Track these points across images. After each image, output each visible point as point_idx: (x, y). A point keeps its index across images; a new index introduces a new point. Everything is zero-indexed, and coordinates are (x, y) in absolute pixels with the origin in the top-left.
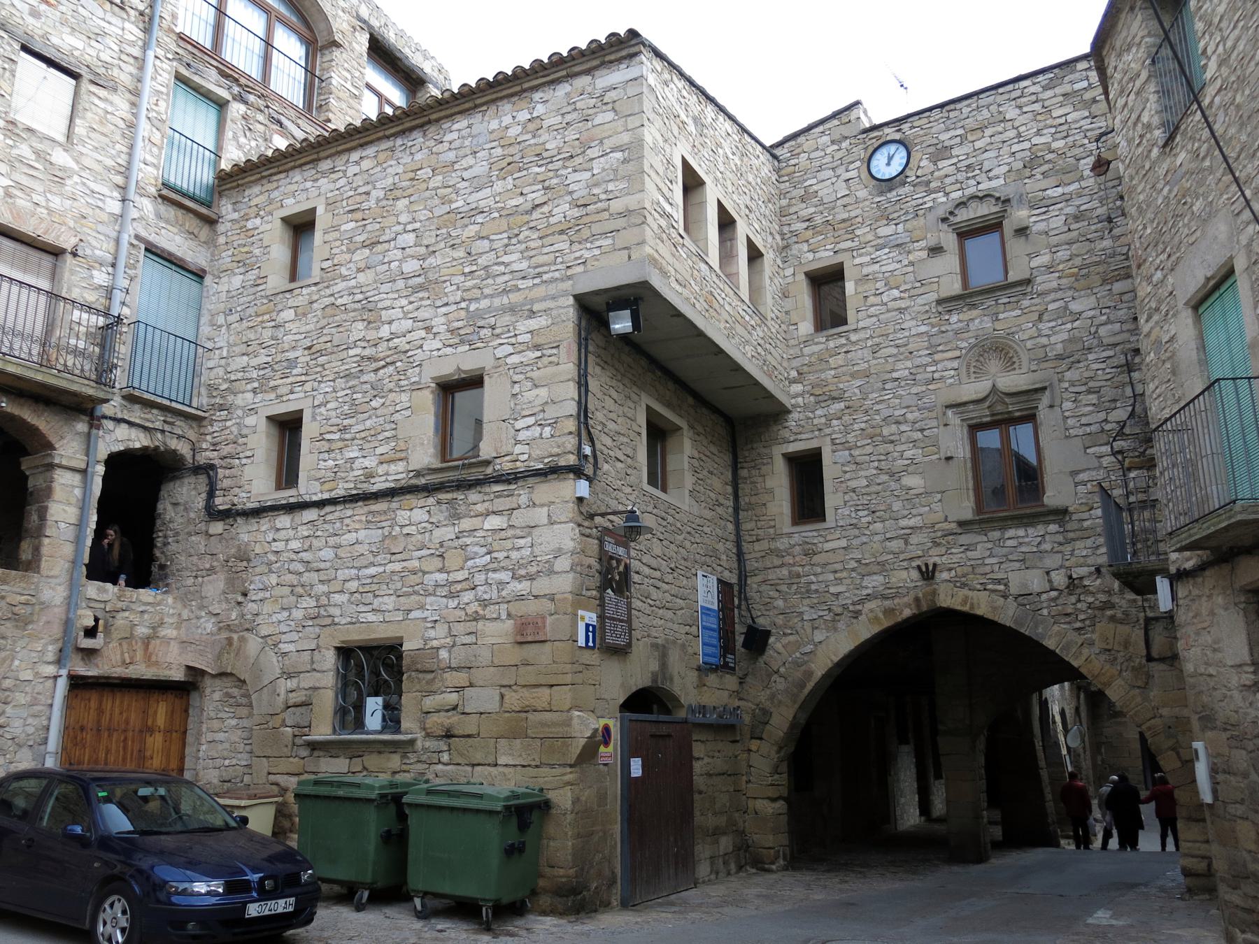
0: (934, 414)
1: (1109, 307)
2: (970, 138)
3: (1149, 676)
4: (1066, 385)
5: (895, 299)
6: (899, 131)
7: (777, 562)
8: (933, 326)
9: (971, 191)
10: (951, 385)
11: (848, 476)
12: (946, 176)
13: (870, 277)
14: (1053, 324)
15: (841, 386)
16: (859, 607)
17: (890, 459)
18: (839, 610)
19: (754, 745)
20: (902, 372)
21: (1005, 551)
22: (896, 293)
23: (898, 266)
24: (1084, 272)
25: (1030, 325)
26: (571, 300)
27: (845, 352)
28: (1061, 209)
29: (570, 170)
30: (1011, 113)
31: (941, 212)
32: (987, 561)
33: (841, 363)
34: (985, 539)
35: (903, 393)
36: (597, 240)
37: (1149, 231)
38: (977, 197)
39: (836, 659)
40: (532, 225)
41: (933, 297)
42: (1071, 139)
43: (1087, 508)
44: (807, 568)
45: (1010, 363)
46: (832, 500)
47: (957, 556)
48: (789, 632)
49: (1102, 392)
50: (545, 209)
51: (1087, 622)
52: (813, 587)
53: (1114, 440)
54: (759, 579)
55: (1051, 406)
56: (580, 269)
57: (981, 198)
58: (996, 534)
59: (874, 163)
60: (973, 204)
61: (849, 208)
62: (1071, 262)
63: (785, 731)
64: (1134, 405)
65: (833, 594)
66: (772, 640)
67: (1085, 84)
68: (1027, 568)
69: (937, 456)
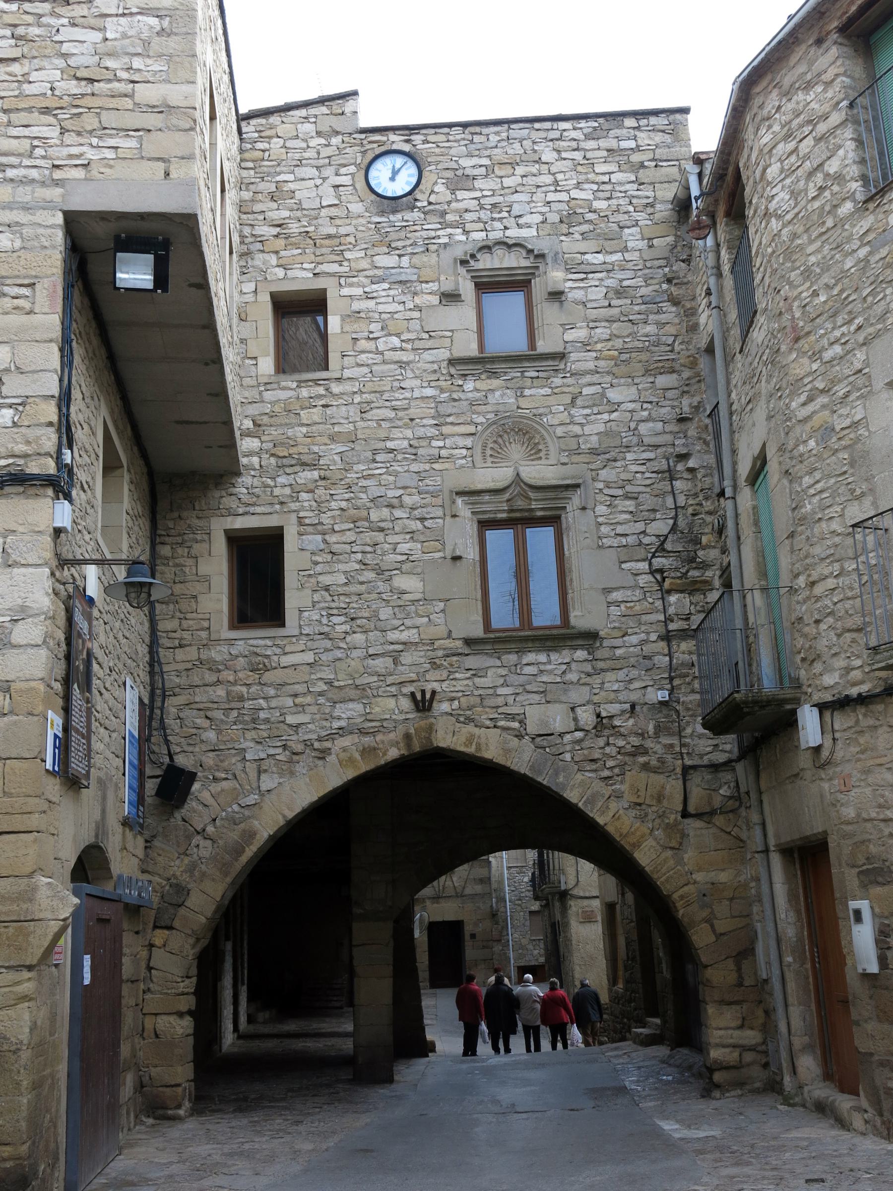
0: (439, 501)
1: (651, 402)
2: (498, 172)
3: (684, 835)
4: (601, 485)
5: (394, 349)
6: (407, 141)
7: (210, 677)
8: (442, 391)
9: (497, 235)
10: (462, 467)
11: (319, 569)
12: (466, 211)
13: (362, 315)
14: (588, 411)
15: (316, 449)
16: (328, 744)
17: (379, 552)
18: (299, 748)
19: (159, 937)
20: (399, 442)
21: (522, 679)
22: (395, 341)
23: (401, 308)
24: (624, 357)
25: (562, 408)
26: (59, 219)
27: (323, 406)
28: (601, 280)
29: (65, 21)
30: (548, 155)
31: (459, 252)
32: (500, 691)
33: (316, 418)
34: (499, 663)
35: (399, 469)
36: (111, 136)
37: (822, 298)
39: (290, 815)
41: (444, 354)
42: (614, 202)
43: (621, 634)
44: (254, 689)
45: (535, 452)
46: (293, 599)
47: (462, 682)
48: (223, 776)
49: (640, 499)
50: (15, 68)
51: (617, 771)
52: (262, 715)
53: (652, 557)
54: (181, 700)
55: (584, 509)
56: (79, 174)
57: (509, 246)
58: (512, 658)
59: (373, 173)
60: (499, 252)
61: (338, 222)
62: (611, 343)
63: (209, 915)
64: (675, 518)
65: (290, 725)
66: (196, 786)
67: (632, 144)
68: (548, 702)
69: (441, 554)
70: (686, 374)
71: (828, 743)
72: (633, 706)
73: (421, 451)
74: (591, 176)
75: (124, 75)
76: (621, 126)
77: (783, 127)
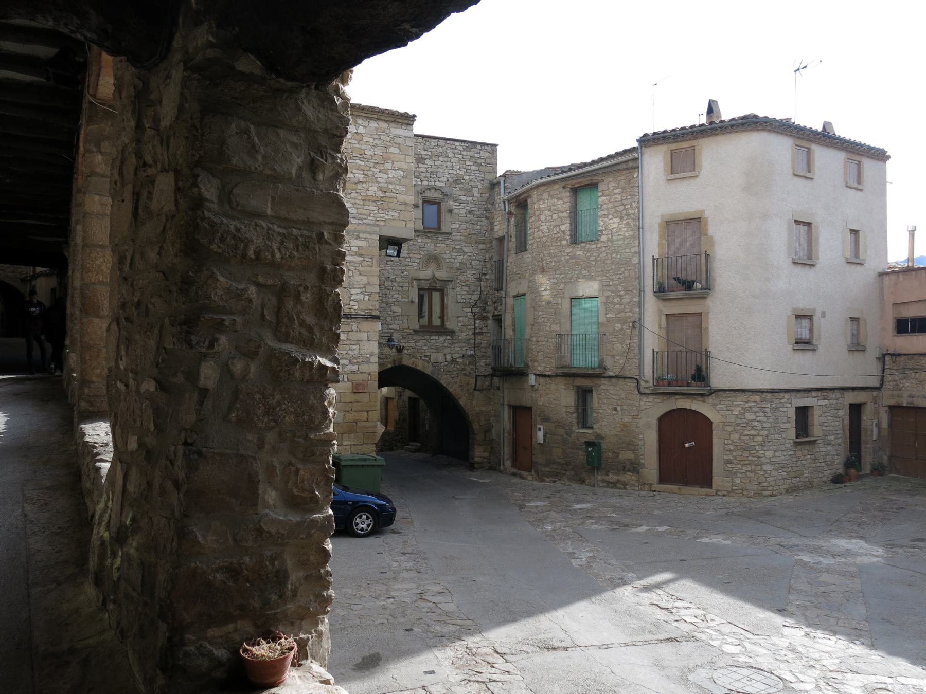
0: (407, 281)
2: (434, 159)
3: (474, 396)
9: (431, 184)
10: (415, 269)
12: (422, 172)
14: (457, 254)
26: (378, 238)
32: (423, 348)
38: (434, 188)
40: (358, 191)
45: (439, 267)
47: (412, 344)
50: (364, 185)
56: (383, 223)
57: (436, 190)
64: (480, 295)
67: (478, 155)
70: (488, 245)
71: (537, 384)
72: (463, 356)
73: (403, 262)
74: (464, 166)
75: (394, 191)
76: (475, 148)
77: (548, 206)
